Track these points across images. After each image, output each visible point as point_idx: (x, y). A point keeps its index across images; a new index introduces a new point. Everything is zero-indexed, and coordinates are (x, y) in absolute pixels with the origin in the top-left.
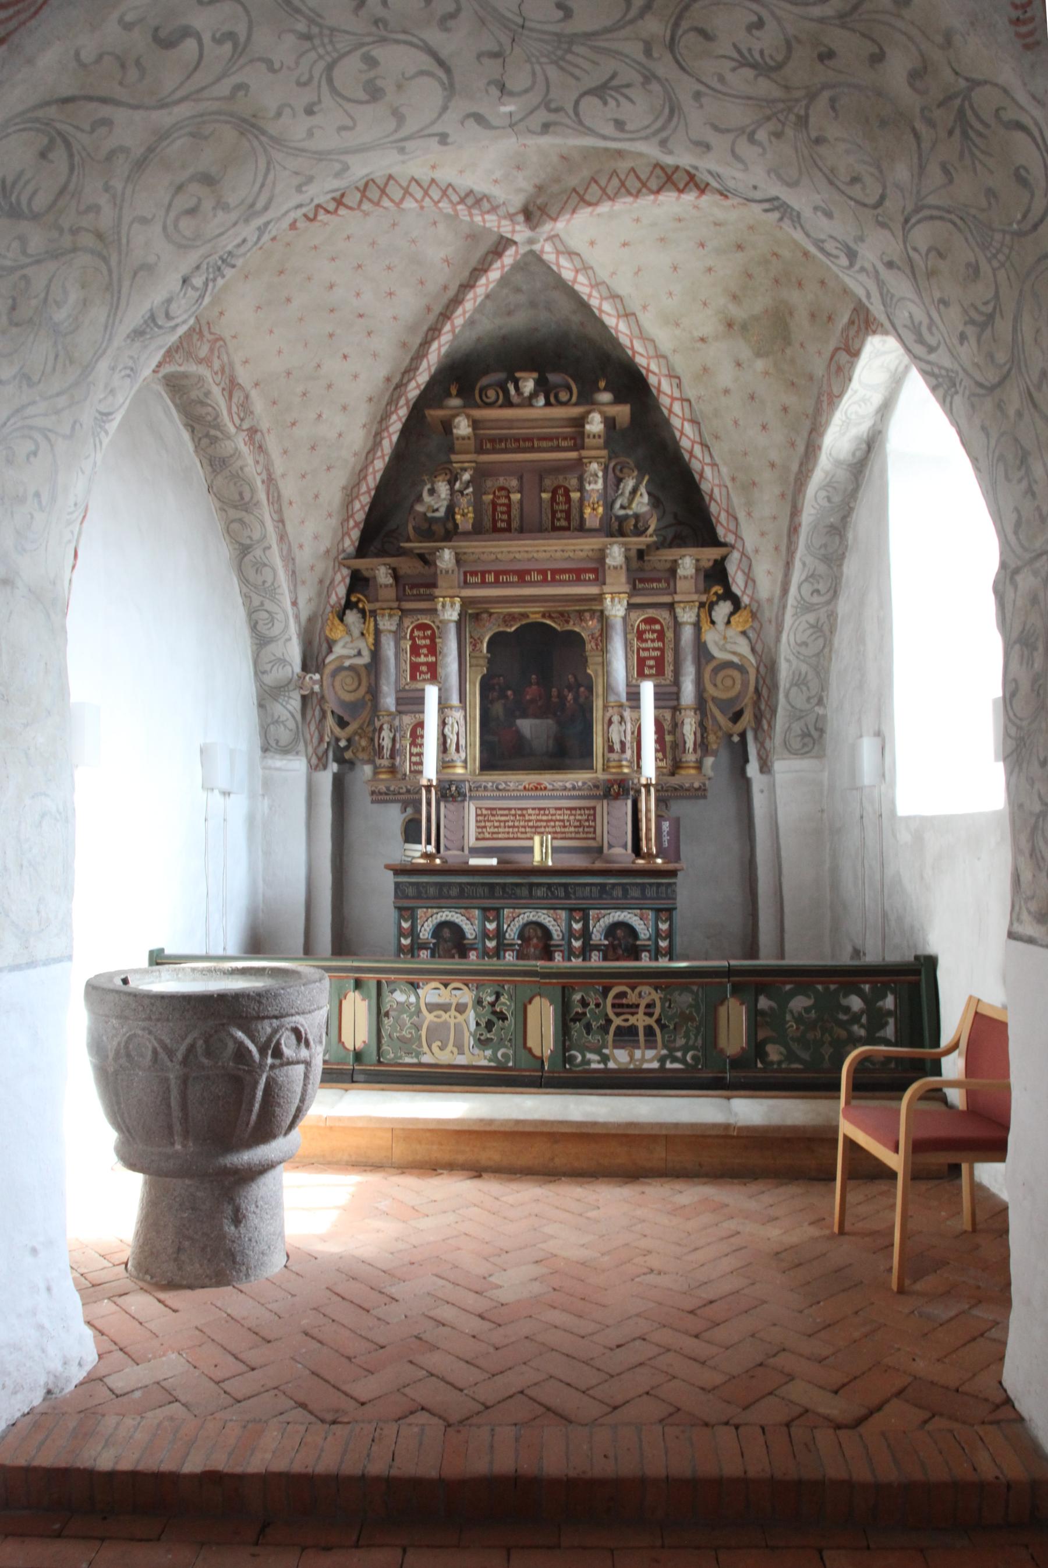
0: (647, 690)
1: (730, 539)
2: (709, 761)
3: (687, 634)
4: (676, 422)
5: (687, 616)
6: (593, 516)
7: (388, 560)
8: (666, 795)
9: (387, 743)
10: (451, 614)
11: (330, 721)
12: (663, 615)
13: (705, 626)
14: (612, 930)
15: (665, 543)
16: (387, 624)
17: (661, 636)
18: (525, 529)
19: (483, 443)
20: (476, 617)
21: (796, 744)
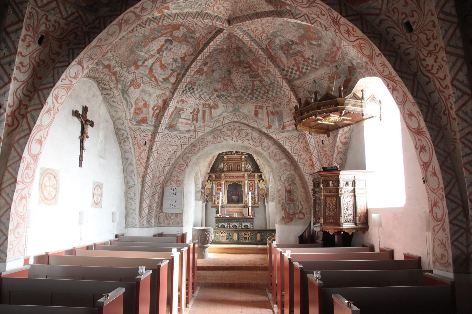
0: (250, 193)
1: (262, 172)
2: (259, 202)
3: (256, 185)
4: (254, 157)
5: (256, 182)
6: (243, 169)
7: (215, 174)
8: (253, 207)
9: (214, 200)
10: (223, 182)
11: (206, 196)
12: (253, 182)
13: (259, 183)
14: (245, 226)
15: (253, 172)
16: (214, 182)
17: (253, 185)
18: (233, 171)
19: (228, 159)
20: (227, 182)
21: (272, 200)
